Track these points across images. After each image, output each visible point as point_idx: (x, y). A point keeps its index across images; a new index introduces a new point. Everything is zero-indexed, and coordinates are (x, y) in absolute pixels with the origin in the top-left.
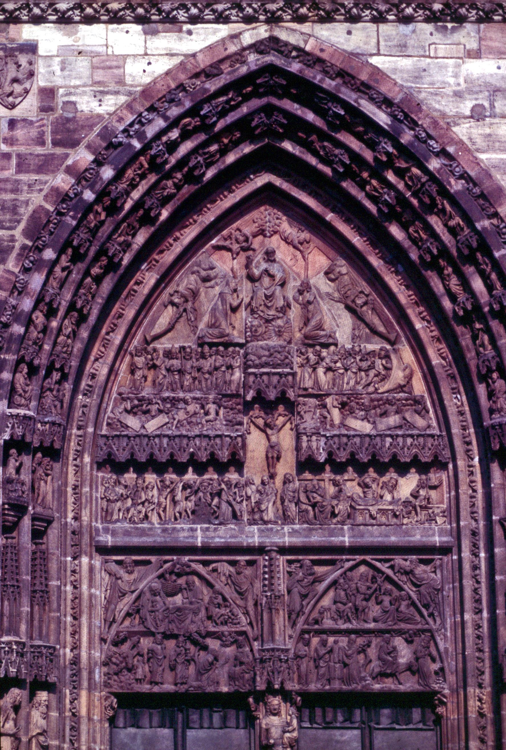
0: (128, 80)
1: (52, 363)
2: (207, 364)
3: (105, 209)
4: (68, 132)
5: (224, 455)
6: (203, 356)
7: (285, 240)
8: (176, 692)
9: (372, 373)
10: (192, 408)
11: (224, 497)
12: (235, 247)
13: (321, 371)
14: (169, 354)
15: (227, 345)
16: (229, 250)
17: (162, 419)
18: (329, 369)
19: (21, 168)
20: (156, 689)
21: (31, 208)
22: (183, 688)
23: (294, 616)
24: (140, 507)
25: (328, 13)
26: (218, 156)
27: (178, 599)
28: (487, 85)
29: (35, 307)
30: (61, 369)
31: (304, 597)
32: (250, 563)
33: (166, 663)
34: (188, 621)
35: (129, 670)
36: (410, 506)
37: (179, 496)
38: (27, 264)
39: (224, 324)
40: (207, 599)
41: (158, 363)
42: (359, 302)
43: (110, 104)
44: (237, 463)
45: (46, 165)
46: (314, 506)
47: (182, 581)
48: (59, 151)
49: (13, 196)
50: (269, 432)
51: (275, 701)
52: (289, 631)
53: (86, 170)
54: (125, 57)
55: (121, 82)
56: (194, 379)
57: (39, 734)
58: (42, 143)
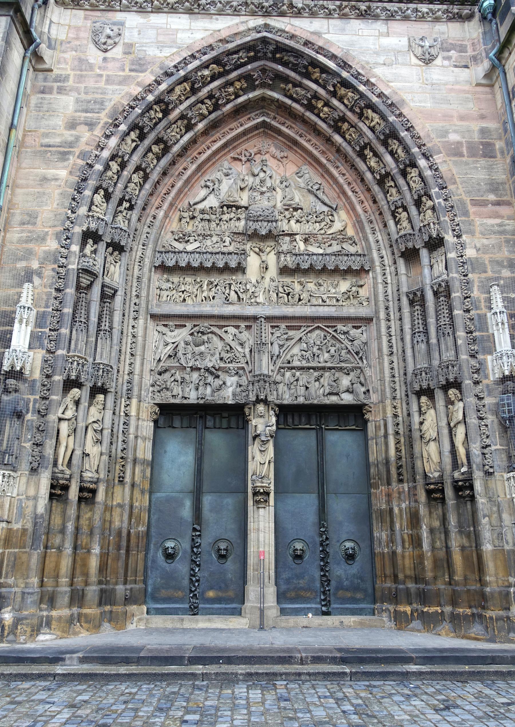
0: (179, 41)
1: (124, 197)
2: (225, 217)
3: (162, 111)
4: (140, 65)
5: (233, 264)
6: (223, 213)
7: (273, 157)
8: (198, 404)
9: (323, 224)
10: (215, 239)
11: (233, 288)
12: (244, 159)
13: (293, 222)
14: (203, 212)
15: (238, 207)
16: (241, 160)
17: (196, 245)
18: (298, 221)
19: (108, 81)
20: (185, 402)
21: (113, 103)
22: (202, 402)
23: (274, 358)
24: (181, 294)
25: (299, 10)
26: (233, 97)
27: (202, 348)
28: (394, 50)
29: (113, 158)
30: (129, 201)
31: (281, 346)
32: (248, 327)
33: (192, 386)
34: (207, 360)
35: (167, 389)
36: (347, 295)
37: (205, 287)
38: (108, 132)
39: (236, 195)
40: (220, 348)
41: (196, 215)
42: (316, 187)
43: (167, 52)
44: (241, 269)
45: (125, 81)
46: (288, 294)
47: (205, 337)
48: (133, 74)
49: (102, 96)
50: (261, 254)
51: (261, 408)
52: (271, 367)
53: (150, 85)
54: (177, 30)
55: (174, 41)
56: (218, 224)
57: (94, 422)
58: (124, 70)
